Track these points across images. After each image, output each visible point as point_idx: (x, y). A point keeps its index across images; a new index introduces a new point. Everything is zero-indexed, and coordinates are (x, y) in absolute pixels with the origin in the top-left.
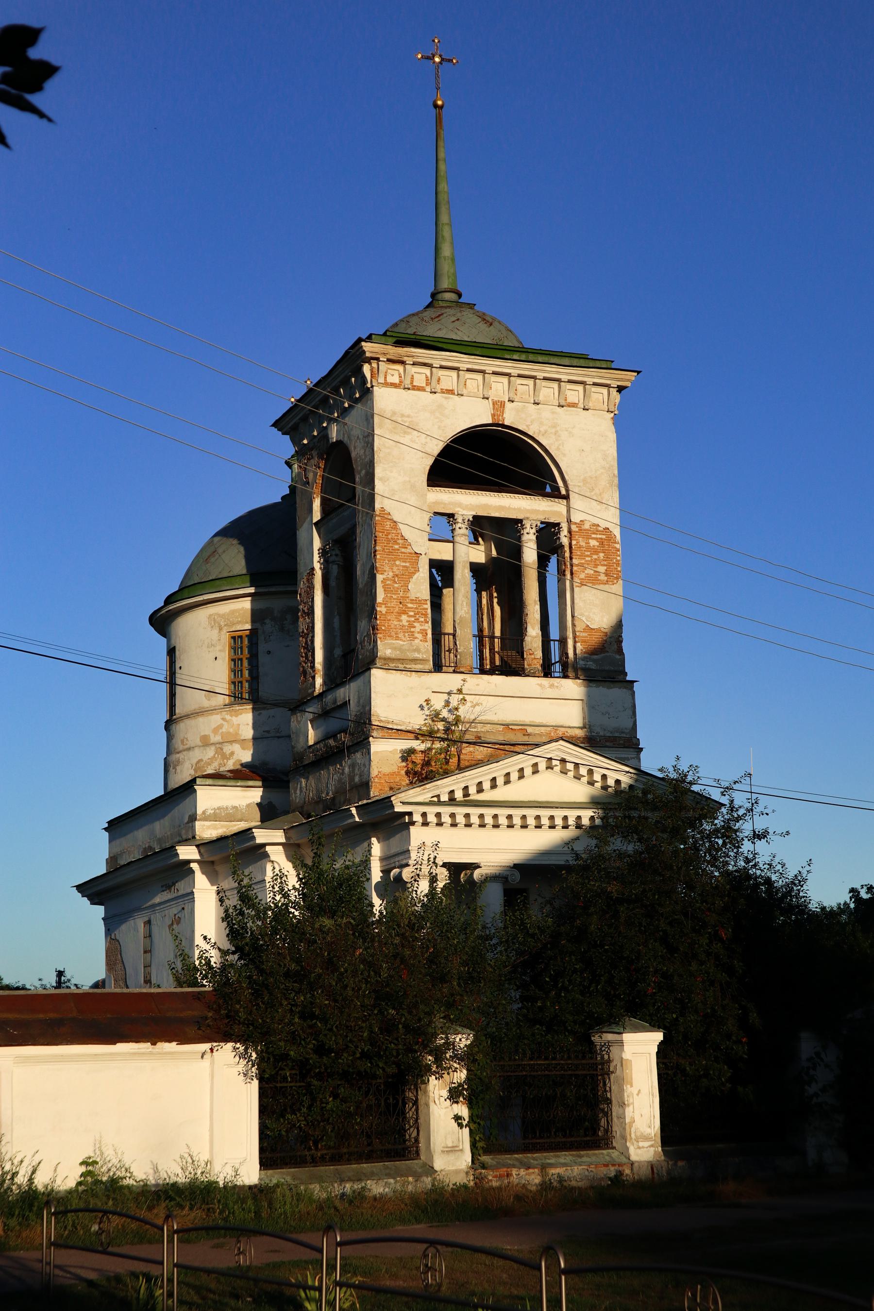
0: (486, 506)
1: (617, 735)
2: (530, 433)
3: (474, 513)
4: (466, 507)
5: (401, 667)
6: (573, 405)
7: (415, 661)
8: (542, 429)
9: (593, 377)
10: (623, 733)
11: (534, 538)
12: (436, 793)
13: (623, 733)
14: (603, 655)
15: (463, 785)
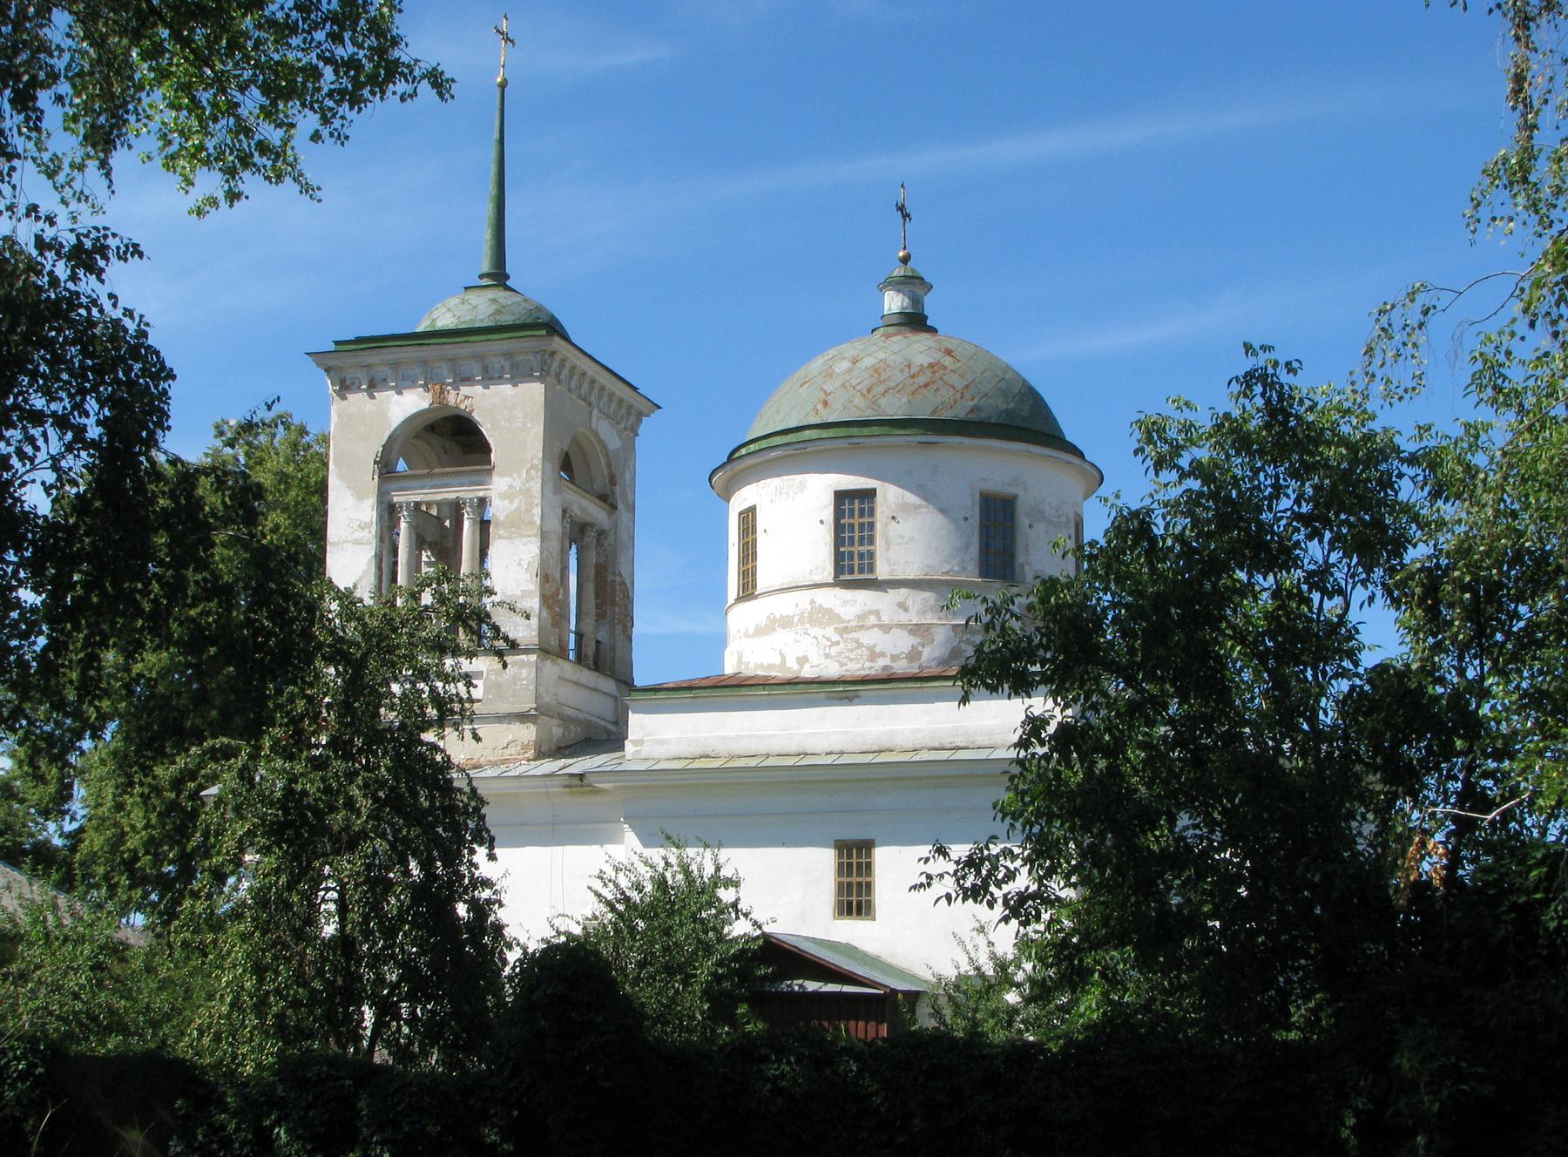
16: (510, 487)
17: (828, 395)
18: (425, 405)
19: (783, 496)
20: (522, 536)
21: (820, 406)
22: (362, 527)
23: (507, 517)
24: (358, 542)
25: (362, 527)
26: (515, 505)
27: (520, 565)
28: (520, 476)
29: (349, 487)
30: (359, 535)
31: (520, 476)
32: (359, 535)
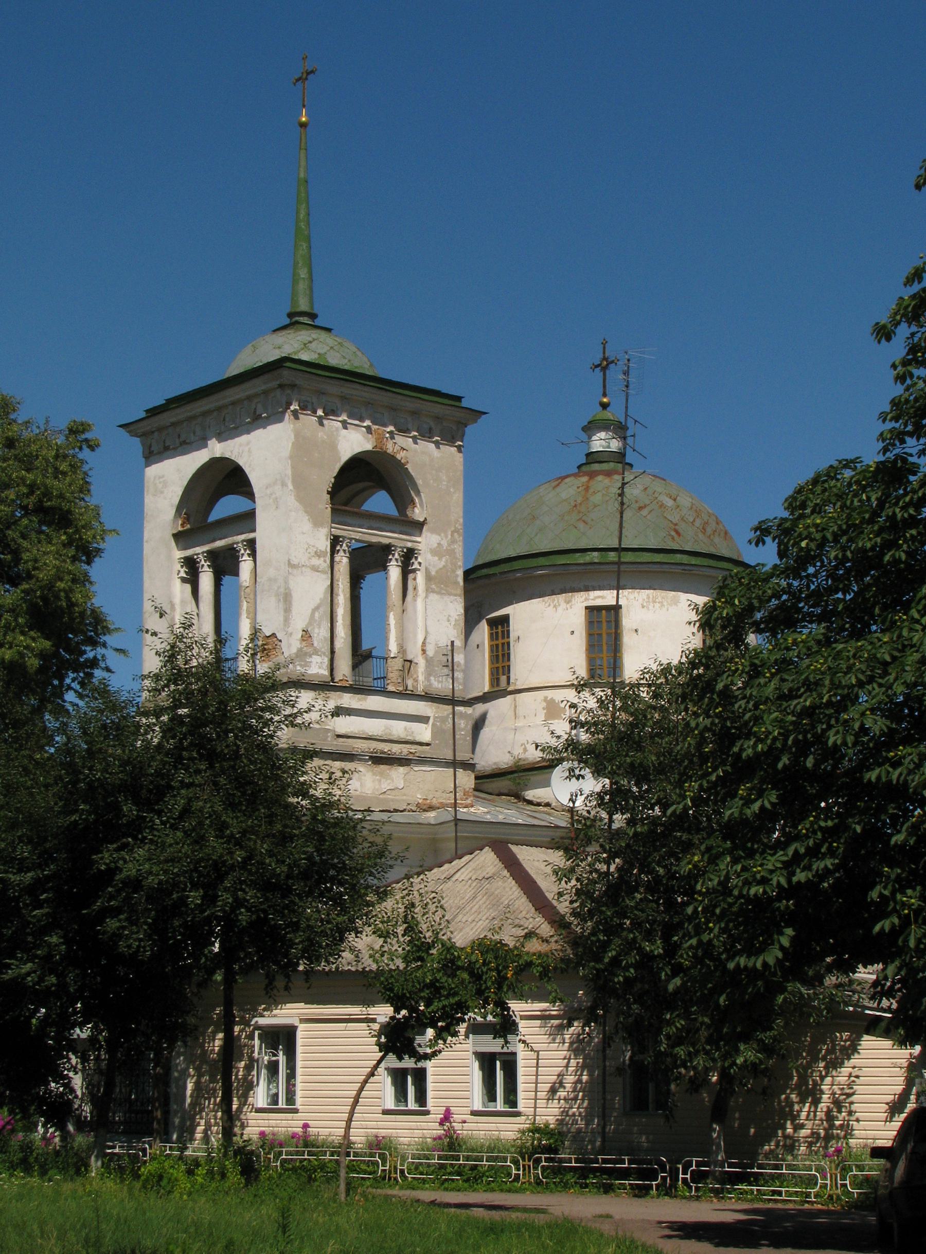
16: (439, 544)
17: (676, 525)
18: (368, 446)
19: (657, 605)
20: (450, 594)
21: (673, 533)
22: (318, 554)
23: (437, 572)
24: (315, 569)
25: (318, 554)
26: (443, 563)
27: (449, 621)
28: (446, 537)
29: (306, 512)
31: (446, 537)
32: (316, 562)
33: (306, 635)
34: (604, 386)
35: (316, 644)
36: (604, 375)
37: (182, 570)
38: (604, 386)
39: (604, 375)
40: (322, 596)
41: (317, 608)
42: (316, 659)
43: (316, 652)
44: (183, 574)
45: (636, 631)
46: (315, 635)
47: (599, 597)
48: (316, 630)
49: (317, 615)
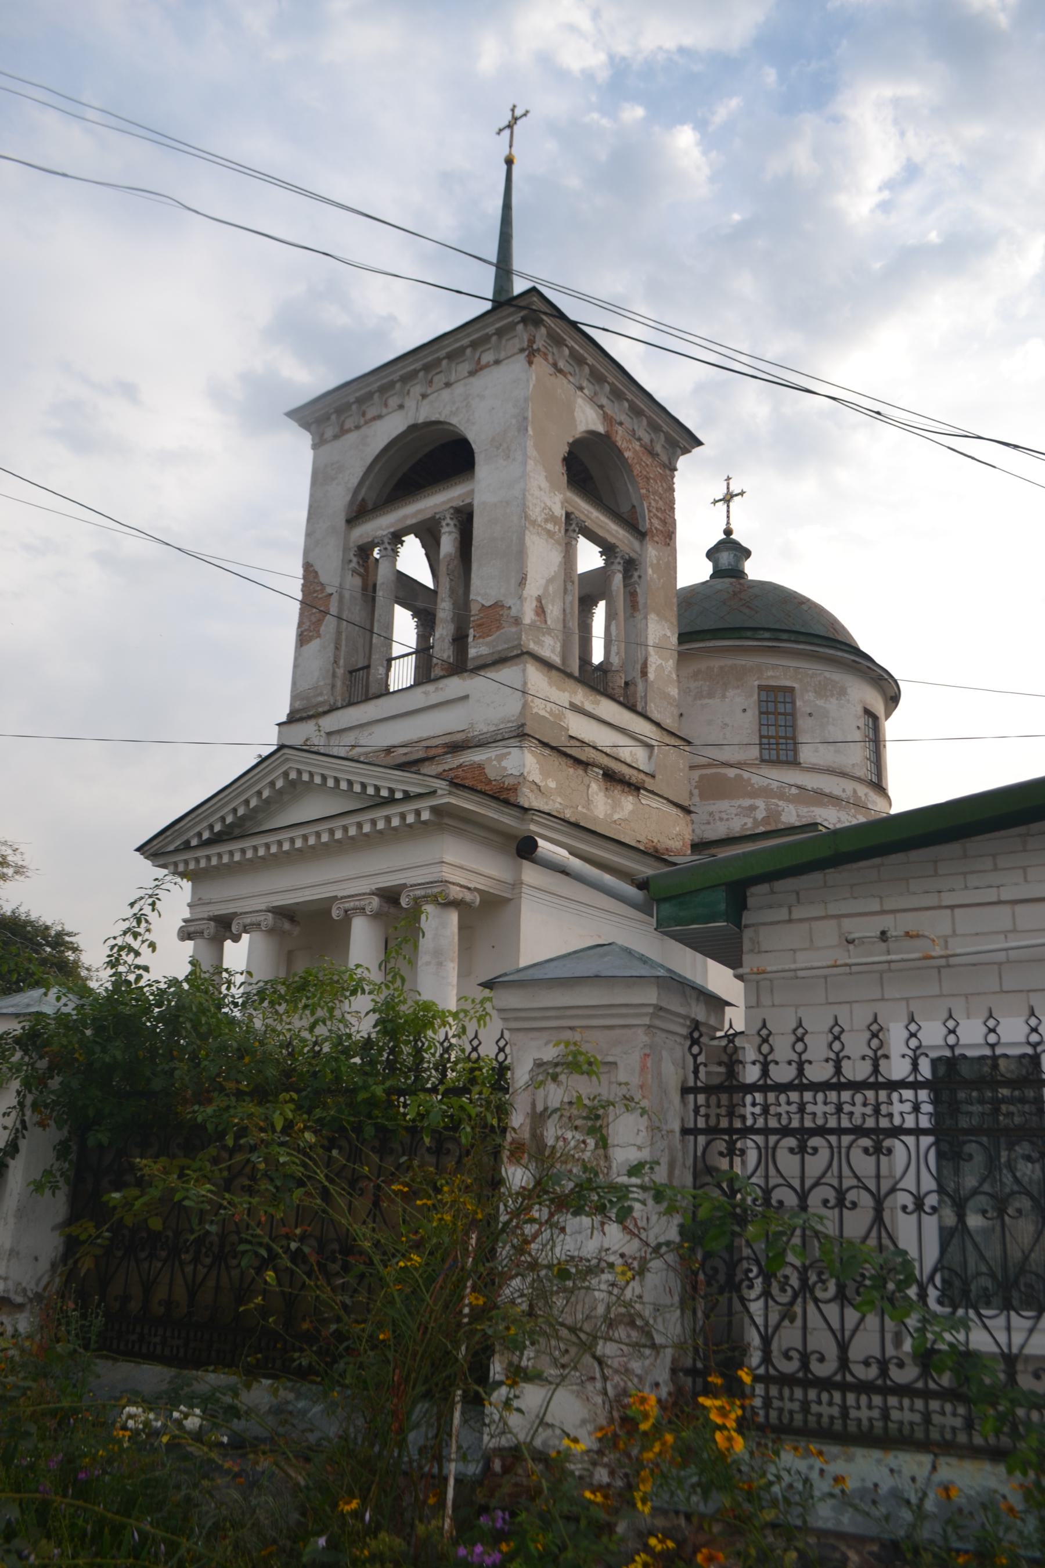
0: (405, 517)
1: (501, 726)
2: (442, 419)
3: (392, 530)
4: (388, 527)
5: (305, 715)
6: (487, 365)
7: (320, 704)
8: (454, 409)
9: (493, 324)
10: (509, 722)
11: (451, 528)
12: (185, 838)
13: (509, 722)
14: (498, 633)
15: (205, 824)
18: (601, 429)
30: (550, 526)
32: (550, 526)
33: (541, 611)
34: (728, 517)
35: (549, 622)
36: (728, 506)
37: (355, 560)
38: (728, 517)
39: (728, 506)
40: (556, 569)
41: (550, 581)
42: (548, 641)
43: (549, 631)
44: (354, 565)
45: (810, 715)
46: (548, 612)
47: (772, 677)
48: (550, 607)
49: (551, 589)
